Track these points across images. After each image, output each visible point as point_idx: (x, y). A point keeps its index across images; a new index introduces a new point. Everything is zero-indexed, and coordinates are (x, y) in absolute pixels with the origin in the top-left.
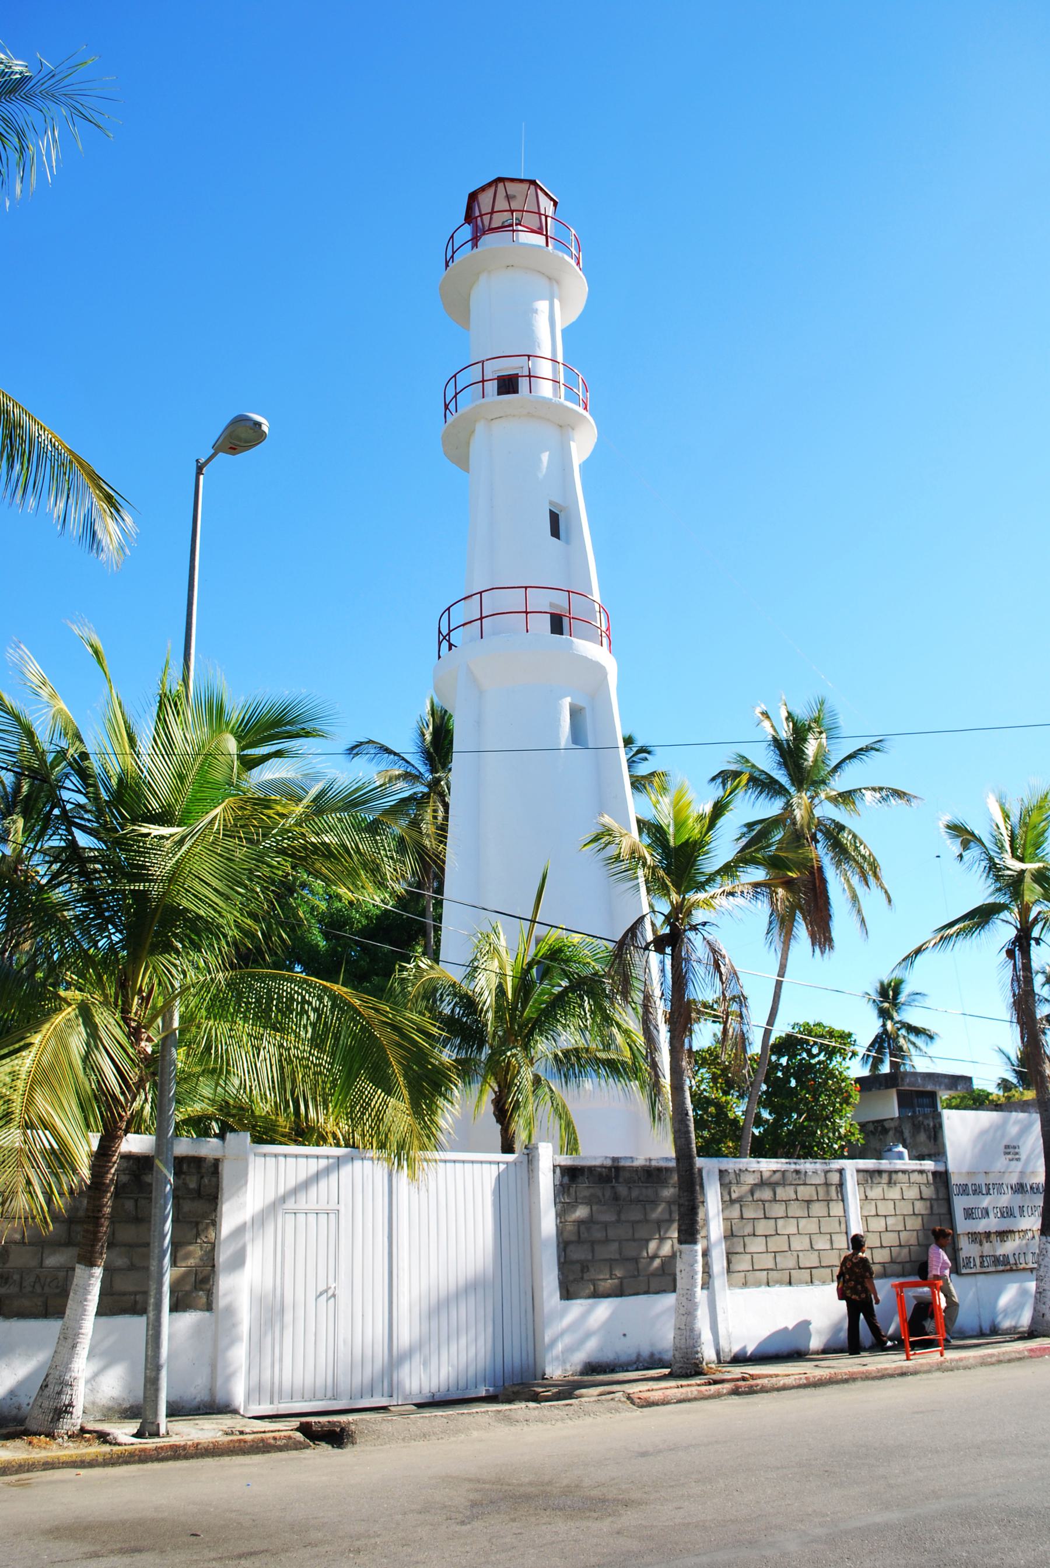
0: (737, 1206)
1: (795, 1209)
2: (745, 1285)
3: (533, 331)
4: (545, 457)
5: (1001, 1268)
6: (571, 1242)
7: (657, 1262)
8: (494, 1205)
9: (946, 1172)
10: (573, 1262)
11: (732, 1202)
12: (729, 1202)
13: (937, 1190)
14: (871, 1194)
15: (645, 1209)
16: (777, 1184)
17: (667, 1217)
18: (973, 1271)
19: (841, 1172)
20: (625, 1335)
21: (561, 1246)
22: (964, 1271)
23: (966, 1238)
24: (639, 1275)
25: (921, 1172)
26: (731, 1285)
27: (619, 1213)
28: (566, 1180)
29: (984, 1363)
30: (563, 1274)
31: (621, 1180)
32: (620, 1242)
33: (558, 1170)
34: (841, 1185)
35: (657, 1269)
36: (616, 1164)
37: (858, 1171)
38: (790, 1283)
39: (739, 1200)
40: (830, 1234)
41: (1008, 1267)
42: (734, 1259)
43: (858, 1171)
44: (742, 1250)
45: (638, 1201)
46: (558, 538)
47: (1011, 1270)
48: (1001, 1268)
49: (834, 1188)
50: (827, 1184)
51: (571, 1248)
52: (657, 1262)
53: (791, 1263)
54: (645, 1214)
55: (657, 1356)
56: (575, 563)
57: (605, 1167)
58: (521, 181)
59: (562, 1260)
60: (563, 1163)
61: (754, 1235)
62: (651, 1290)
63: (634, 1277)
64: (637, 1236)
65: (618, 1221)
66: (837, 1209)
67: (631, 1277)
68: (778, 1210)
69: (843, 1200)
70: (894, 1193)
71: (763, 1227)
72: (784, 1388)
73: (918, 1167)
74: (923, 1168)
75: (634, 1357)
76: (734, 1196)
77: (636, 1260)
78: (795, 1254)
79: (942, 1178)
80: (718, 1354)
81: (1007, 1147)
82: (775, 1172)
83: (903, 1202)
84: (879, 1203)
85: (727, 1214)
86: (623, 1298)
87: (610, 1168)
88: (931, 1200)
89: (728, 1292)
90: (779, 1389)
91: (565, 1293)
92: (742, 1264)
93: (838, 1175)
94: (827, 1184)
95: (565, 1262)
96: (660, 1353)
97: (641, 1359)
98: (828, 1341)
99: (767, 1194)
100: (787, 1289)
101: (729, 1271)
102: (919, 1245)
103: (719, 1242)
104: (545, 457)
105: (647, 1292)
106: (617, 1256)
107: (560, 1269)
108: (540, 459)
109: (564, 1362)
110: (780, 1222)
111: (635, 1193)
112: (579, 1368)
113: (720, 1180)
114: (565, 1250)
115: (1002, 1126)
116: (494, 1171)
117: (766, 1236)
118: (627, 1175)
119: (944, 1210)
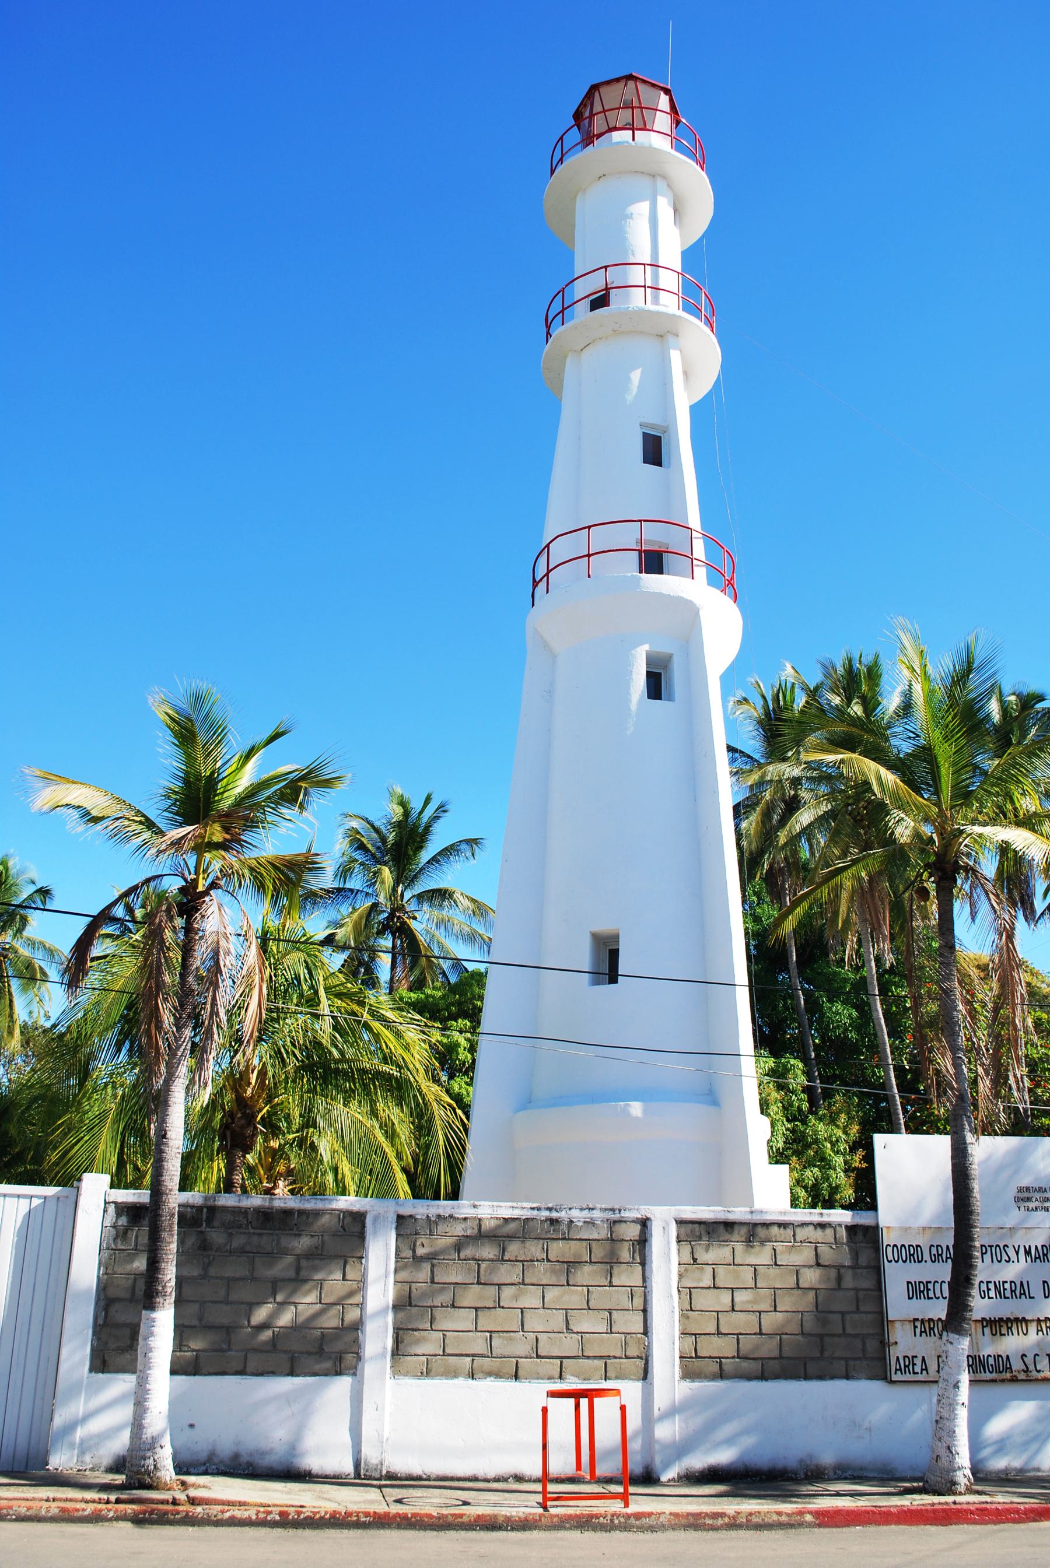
0: (427, 1266)
1: (541, 1272)
2: (428, 1373)
3: (625, 239)
4: (636, 376)
5: (988, 1376)
6: (118, 1300)
7: (267, 1335)
8: (17, 1246)
9: (877, 1227)
10: (118, 1326)
11: (417, 1260)
12: (408, 1258)
13: (855, 1255)
14: (703, 1256)
15: (253, 1263)
16: (511, 1237)
17: (291, 1274)
18: (919, 1377)
19: (644, 1223)
20: (192, 1426)
21: (102, 1303)
22: (894, 1378)
23: (909, 1327)
24: (229, 1349)
25: (822, 1226)
26: (397, 1370)
27: (206, 1267)
28: (123, 1221)
29: (694, 1523)
30: (99, 1339)
31: (216, 1223)
32: (202, 1303)
33: (112, 1209)
34: (643, 1242)
35: (266, 1343)
36: (210, 1203)
37: (680, 1222)
38: (516, 1377)
39: (431, 1257)
40: (610, 1312)
41: (1008, 1375)
42: (408, 1337)
43: (680, 1222)
44: (428, 1326)
45: (242, 1251)
46: (661, 465)
47: (1014, 1380)
48: (988, 1376)
49: (626, 1245)
50: (613, 1241)
51: (117, 1306)
52: (267, 1335)
53: (521, 1346)
54: (253, 1270)
55: (245, 1459)
56: (673, 492)
57: (192, 1207)
58: (618, 80)
59: (101, 1322)
60: (120, 1200)
61: (453, 1306)
62: (248, 1370)
63: (222, 1350)
64: (233, 1297)
65: (204, 1276)
66: (628, 1276)
67: (215, 1350)
68: (508, 1273)
69: (643, 1264)
70: (762, 1256)
71: (472, 1296)
72: (233, 1522)
73: (816, 1219)
74: (825, 1219)
75: (203, 1456)
76: (420, 1251)
77: (228, 1330)
78: (532, 1336)
79: (865, 1238)
80: (357, 1465)
81: (1020, 1190)
82: (506, 1220)
83: (774, 1271)
84: (721, 1270)
85: (404, 1275)
86: (197, 1378)
87: (199, 1209)
88: (839, 1267)
89: (389, 1382)
90: (218, 1523)
91: (98, 1362)
92: (430, 1344)
93: (638, 1227)
94: (613, 1241)
95: (105, 1324)
96: (251, 1454)
97: (216, 1460)
98: (732, 1463)
99: (488, 1251)
100: (511, 1385)
101: (396, 1352)
102: (802, 1333)
103: (383, 1311)
104: (636, 376)
105: (241, 1372)
106: (195, 1322)
107: (94, 1333)
108: (628, 380)
109: (82, 1453)
110: (507, 1292)
111: (238, 1241)
112: (106, 1461)
113: (397, 1228)
114: (106, 1309)
115: (1018, 1158)
116: (24, 1206)
117: (476, 1309)
118: (229, 1217)
119: (867, 1283)
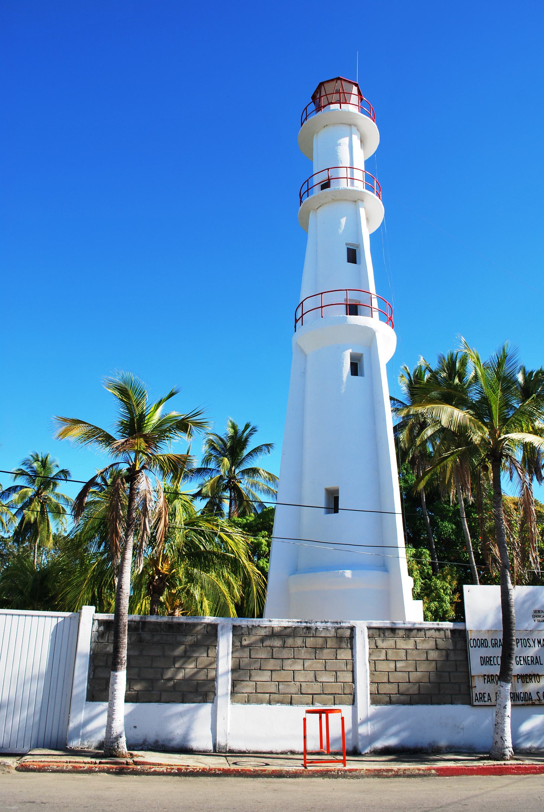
0: (247, 650)
3: (337, 155)
4: (343, 221)
5: (521, 702)
12: (238, 647)
13: (455, 643)
14: (380, 644)
16: (288, 636)
18: (487, 703)
19: (352, 629)
20: (135, 727)
21: (92, 668)
22: (475, 704)
23: (482, 679)
24: (153, 690)
25: (439, 630)
26: (233, 701)
28: (102, 628)
29: (378, 774)
30: (90, 685)
33: (96, 623)
34: (352, 638)
36: (143, 620)
38: (291, 704)
40: (336, 672)
41: (530, 702)
43: (369, 628)
44: (248, 679)
47: (533, 704)
48: (521, 702)
52: (172, 683)
55: (161, 743)
56: (362, 276)
57: (135, 622)
58: (332, 80)
59: (91, 677)
60: (100, 619)
61: (260, 669)
62: (162, 700)
68: (286, 653)
70: (410, 644)
72: (155, 773)
73: (436, 626)
74: (440, 626)
75: (141, 741)
76: (245, 643)
79: (460, 636)
80: (215, 746)
81: (535, 612)
82: (285, 628)
83: (415, 652)
84: (390, 652)
85: (237, 655)
87: (138, 622)
88: (447, 650)
90: (148, 774)
92: (248, 687)
95: (94, 678)
96: (164, 741)
97: (147, 743)
99: (277, 643)
102: (430, 682)
104: (343, 221)
106: (136, 677)
108: (340, 223)
109: (83, 740)
111: (157, 638)
113: (233, 632)
116: (54, 621)
